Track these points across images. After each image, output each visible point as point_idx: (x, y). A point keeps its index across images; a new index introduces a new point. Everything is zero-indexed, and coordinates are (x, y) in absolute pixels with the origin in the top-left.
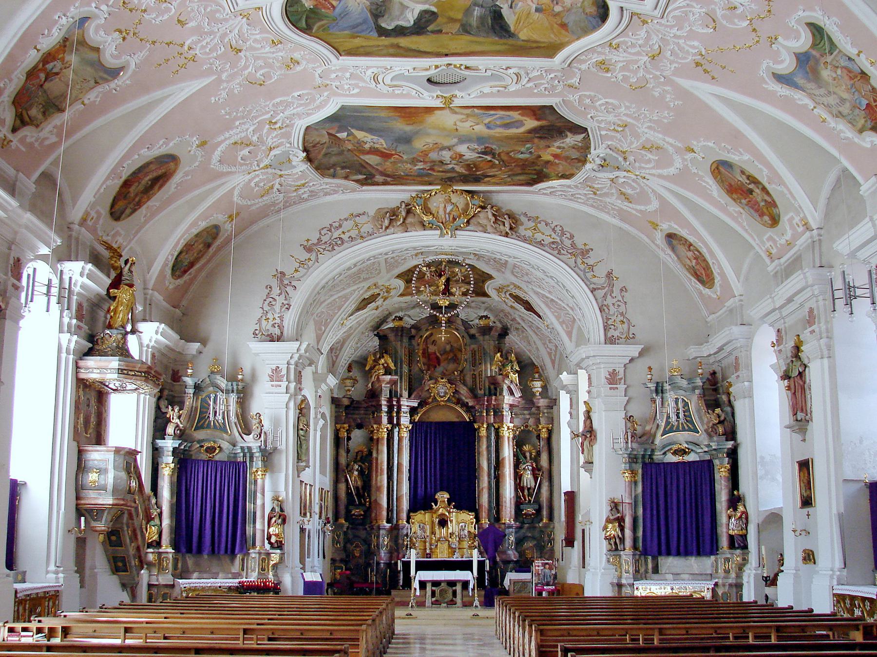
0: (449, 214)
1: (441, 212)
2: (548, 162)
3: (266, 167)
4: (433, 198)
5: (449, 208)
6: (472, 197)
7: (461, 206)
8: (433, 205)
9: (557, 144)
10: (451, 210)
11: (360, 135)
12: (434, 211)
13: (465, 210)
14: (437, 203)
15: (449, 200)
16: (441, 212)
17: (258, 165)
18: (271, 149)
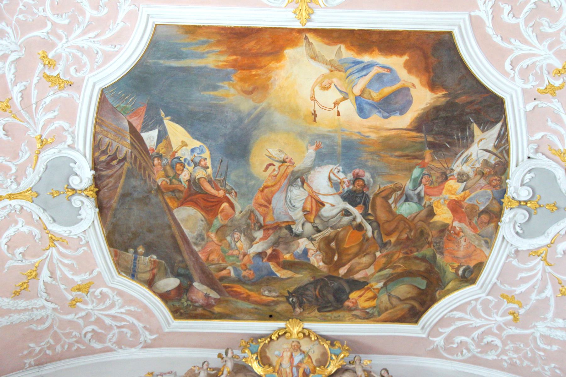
0: (298, 367)
1: (286, 364)
2: (444, 229)
3: (33, 195)
4: (273, 344)
5: (297, 358)
6: (332, 344)
7: (315, 356)
8: (273, 354)
9: (458, 167)
10: (301, 362)
11: (177, 133)
12: (274, 361)
13: (323, 362)
14: (279, 352)
15: (298, 348)
16: (286, 364)
17: (17, 180)
18: (44, 144)
